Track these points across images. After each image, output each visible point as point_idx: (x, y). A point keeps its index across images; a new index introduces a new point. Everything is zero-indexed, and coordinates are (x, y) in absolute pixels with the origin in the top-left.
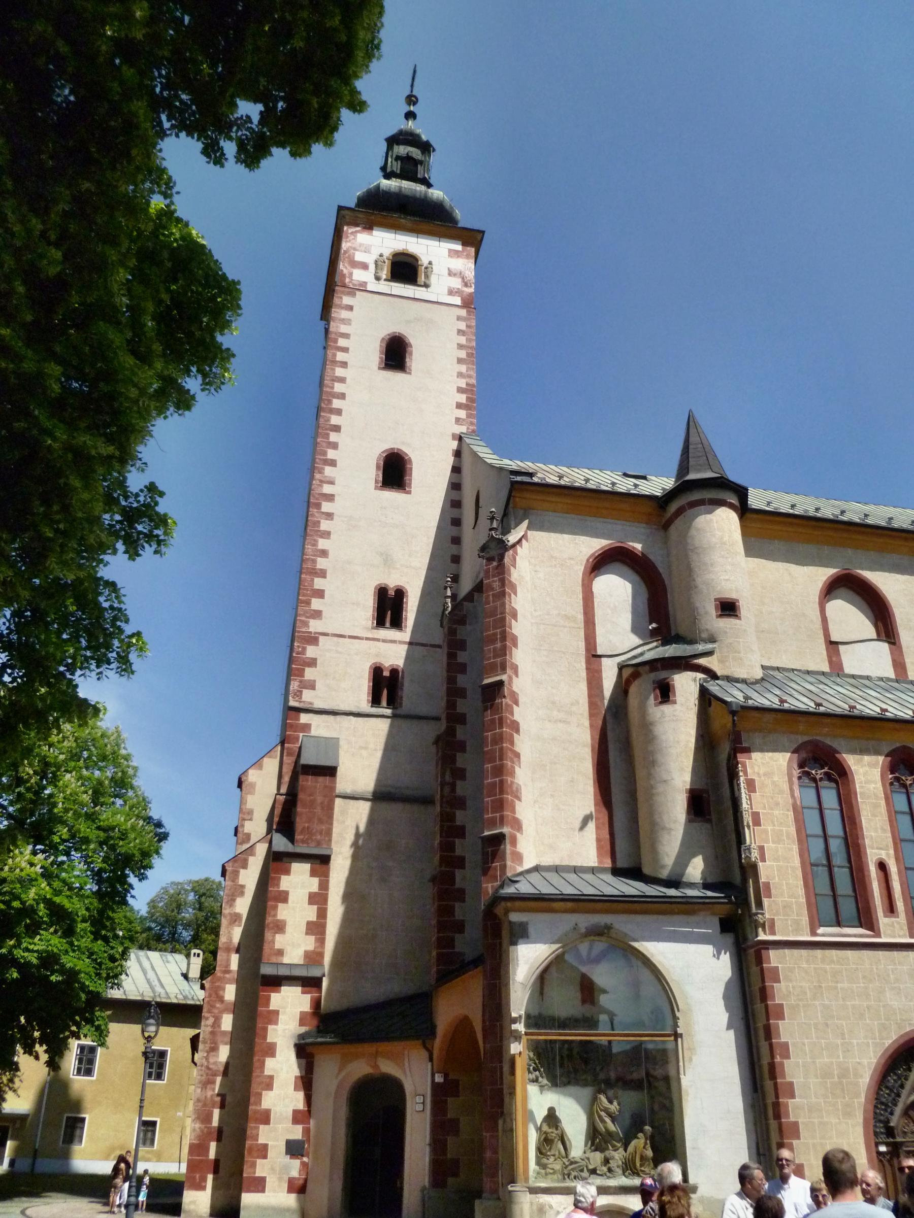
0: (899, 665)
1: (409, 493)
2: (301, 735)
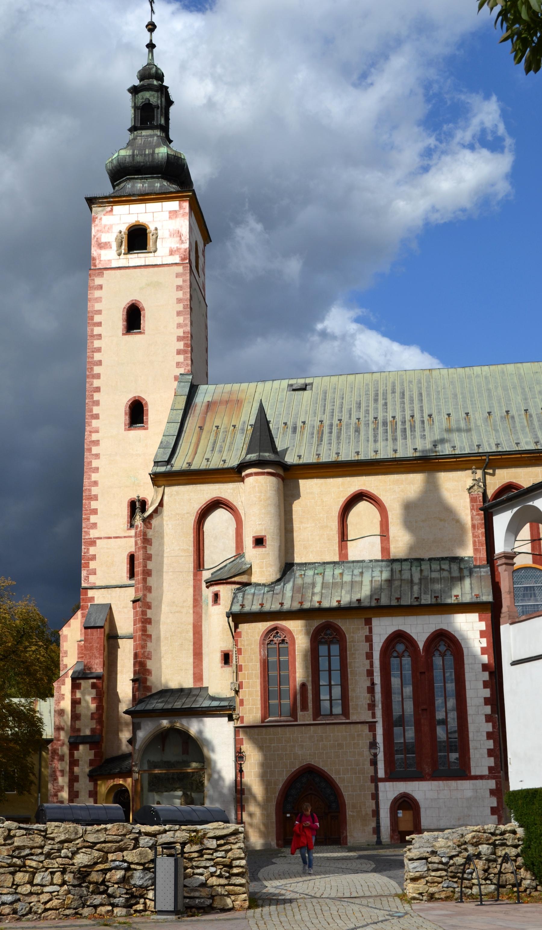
1: (147, 429)
2: (89, 604)
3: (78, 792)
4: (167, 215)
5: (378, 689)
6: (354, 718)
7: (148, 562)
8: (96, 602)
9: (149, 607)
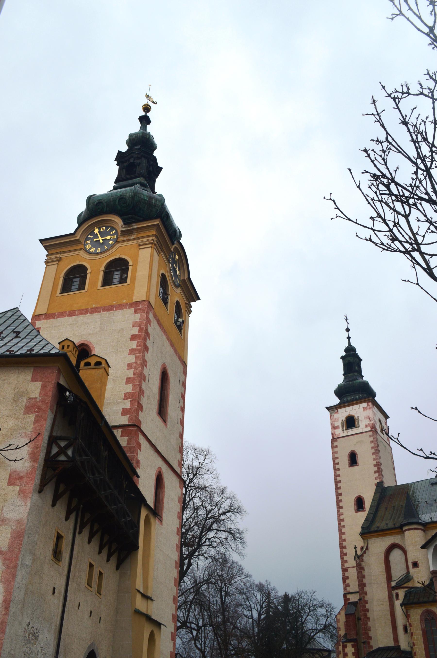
4: (362, 409)
7: (364, 579)
8: (351, 601)
9: (367, 603)
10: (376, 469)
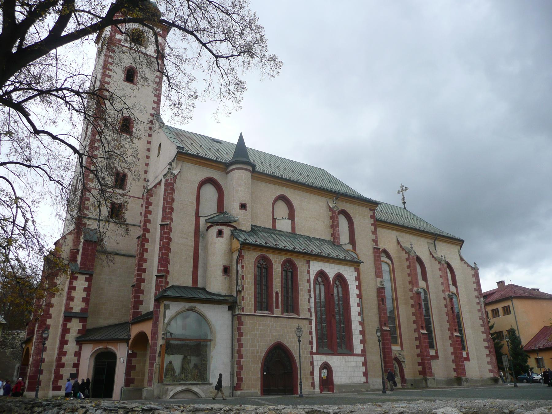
0: (293, 228)
3: (66, 352)
5: (312, 300)
6: (302, 316)
10: (156, 99)
